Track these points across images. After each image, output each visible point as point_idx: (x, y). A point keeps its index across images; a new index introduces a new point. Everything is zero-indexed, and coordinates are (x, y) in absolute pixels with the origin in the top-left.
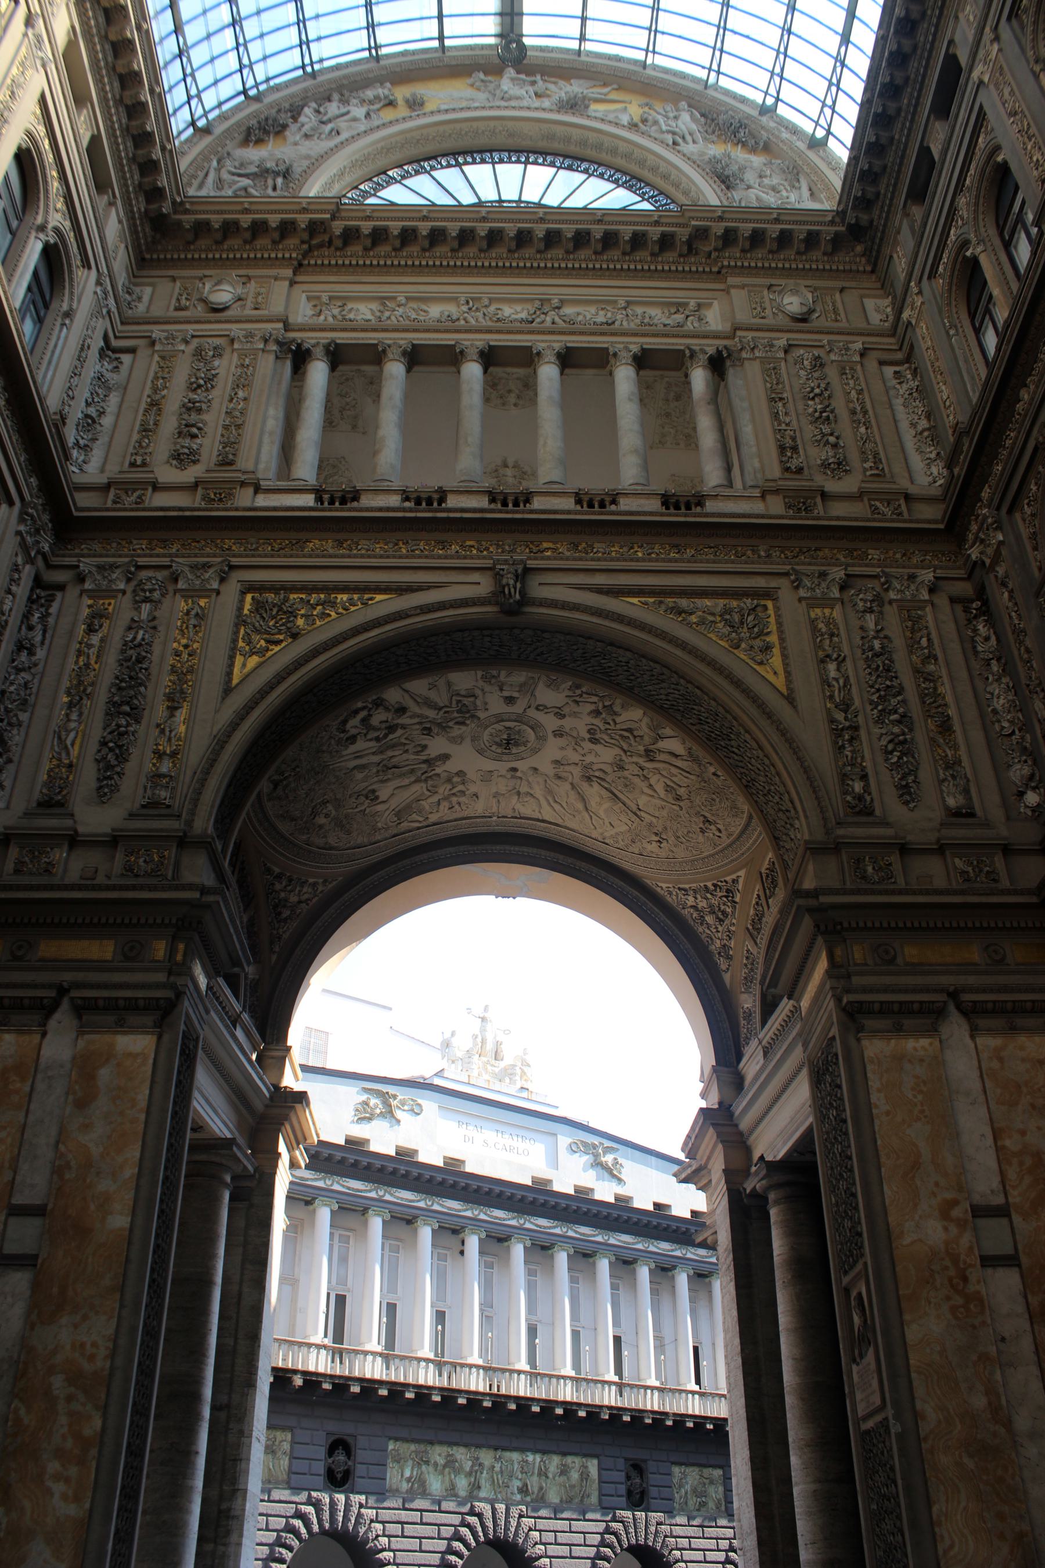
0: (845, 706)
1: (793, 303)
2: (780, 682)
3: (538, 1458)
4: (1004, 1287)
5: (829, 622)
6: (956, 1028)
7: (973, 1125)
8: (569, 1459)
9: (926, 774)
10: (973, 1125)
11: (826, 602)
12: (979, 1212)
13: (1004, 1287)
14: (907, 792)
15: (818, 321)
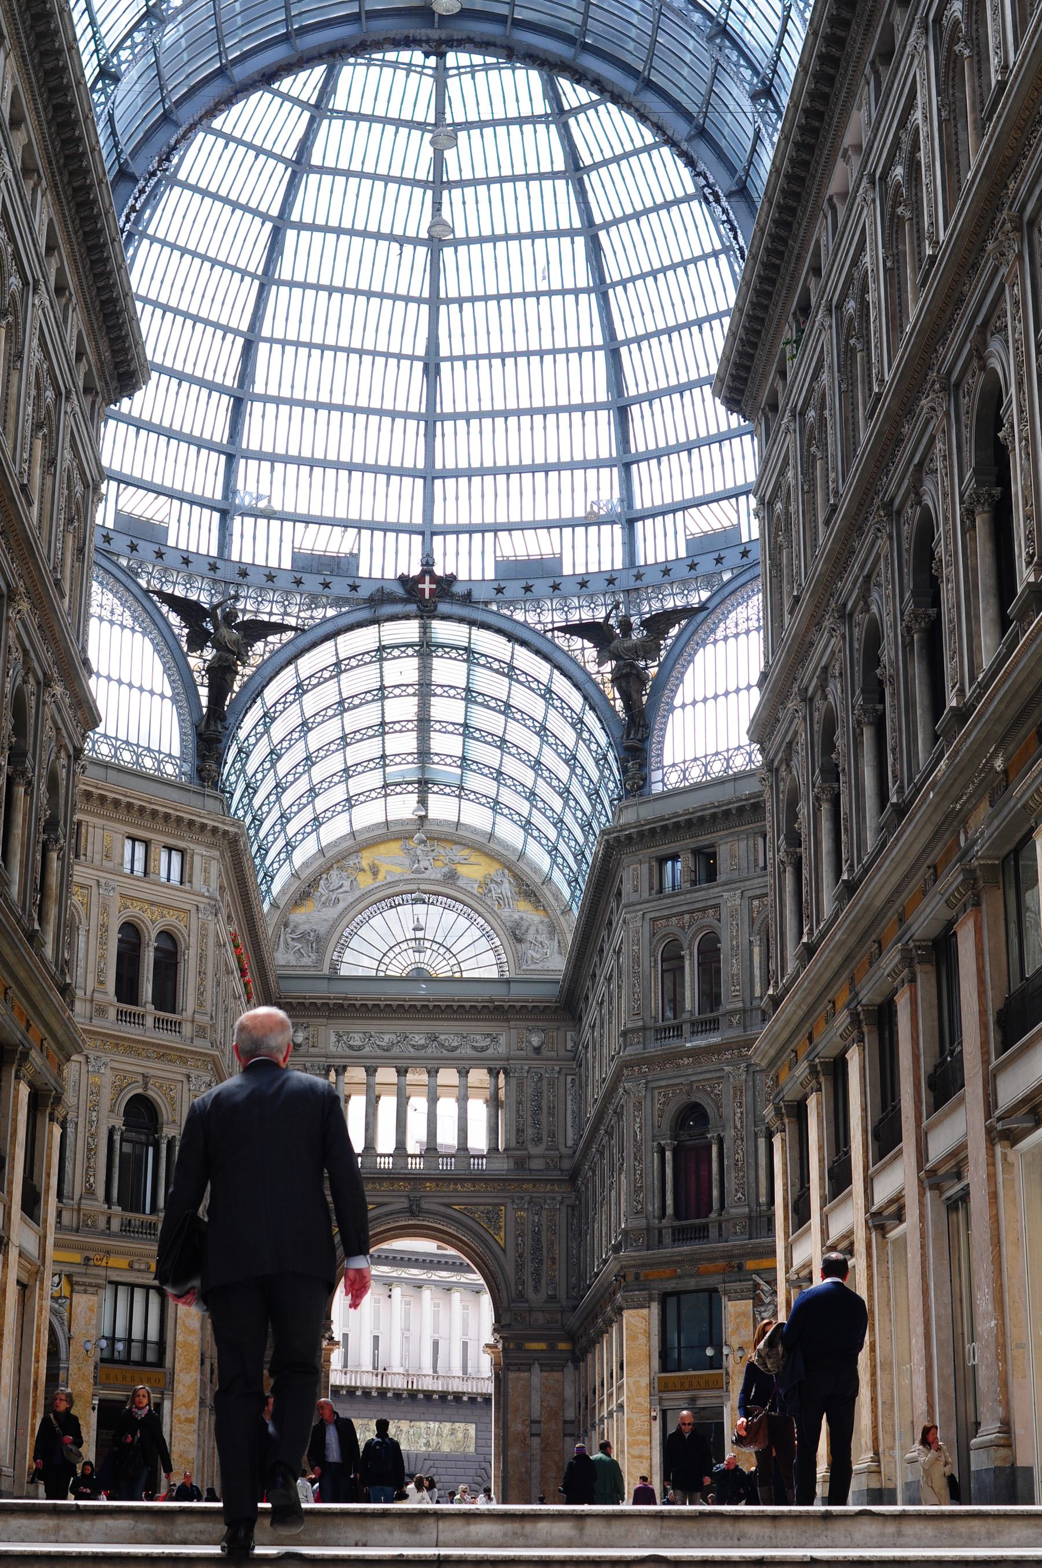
0: (521, 1256)
1: (535, 1040)
2: (502, 1243)
3: (437, 1424)
4: (536, 1442)
5: (521, 1217)
6: (536, 1368)
7: (536, 1398)
8: (457, 1425)
9: (543, 1282)
10: (536, 1398)
11: (521, 1209)
12: (532, 1422)
13: (536, 1442)
14: (536, 1289)
15: (545, 1052)
